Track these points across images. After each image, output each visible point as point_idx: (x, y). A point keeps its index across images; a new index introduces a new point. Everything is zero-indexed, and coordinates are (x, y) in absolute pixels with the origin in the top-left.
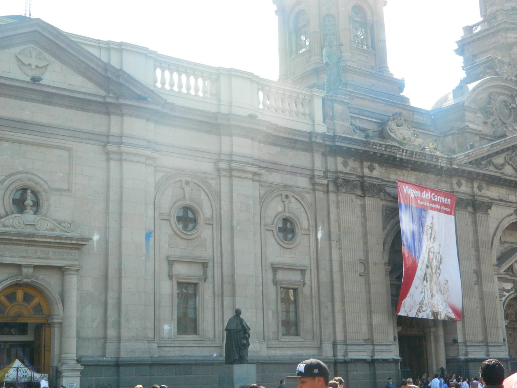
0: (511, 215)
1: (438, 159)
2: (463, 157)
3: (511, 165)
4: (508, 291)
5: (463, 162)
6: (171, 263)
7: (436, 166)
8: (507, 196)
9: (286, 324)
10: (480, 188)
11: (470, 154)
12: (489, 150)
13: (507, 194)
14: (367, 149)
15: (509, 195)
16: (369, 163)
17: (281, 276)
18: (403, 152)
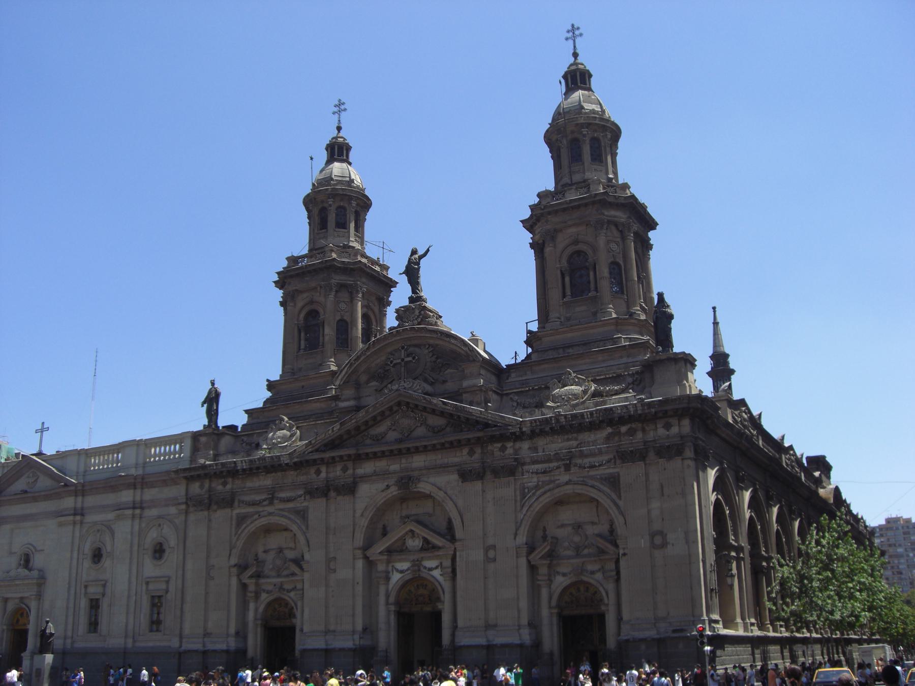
0: (388, 487)
1: (280, 458)
2: (304, 447)
3: (394, 430)
4: (402, 572)
5: (306, 452)
6: (86, 587)
7: (280, 465)
8: (388, 467)
9: (152, 622)
10: (345, 469)
11: (313, 442)
12: (339, 430)
13: (387, 465)
14: (207, 472)
15: (389, 466)
16: (223, 480)
17: (151, 587)
18: (242, 463)
